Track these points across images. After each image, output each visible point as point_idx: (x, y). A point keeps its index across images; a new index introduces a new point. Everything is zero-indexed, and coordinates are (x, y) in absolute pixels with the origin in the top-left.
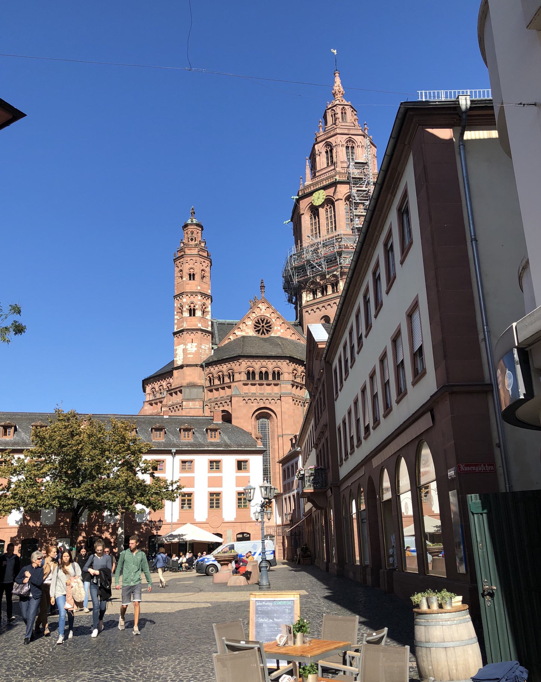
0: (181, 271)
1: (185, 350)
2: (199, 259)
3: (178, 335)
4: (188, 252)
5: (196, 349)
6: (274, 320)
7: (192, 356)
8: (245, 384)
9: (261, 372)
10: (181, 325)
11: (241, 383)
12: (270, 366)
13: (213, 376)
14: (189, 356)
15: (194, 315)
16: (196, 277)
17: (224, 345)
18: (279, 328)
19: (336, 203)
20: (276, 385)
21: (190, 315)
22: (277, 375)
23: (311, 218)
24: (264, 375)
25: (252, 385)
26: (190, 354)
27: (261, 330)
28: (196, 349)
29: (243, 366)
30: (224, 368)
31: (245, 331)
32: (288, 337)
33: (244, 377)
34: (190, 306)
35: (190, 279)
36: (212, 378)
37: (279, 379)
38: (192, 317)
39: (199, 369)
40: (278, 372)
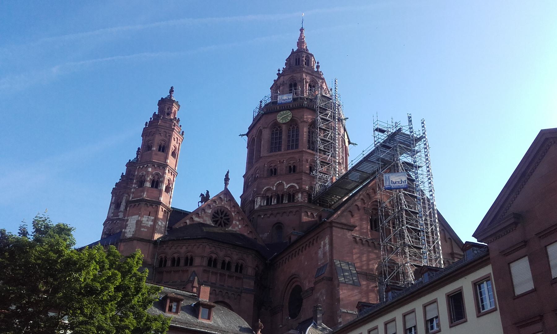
1: (139, 223)
5: (151, 223)
6: (233, 214)
7: (146, 230)
8: (205, 271)
9: (224, 262)
12: (235, 256)
14: (142, 229)
17: (180, 228)
18: (238, 223)
20: (238, 278)
21: (152, 186)
22: (240, 268)
24: (226, 266)
25: (213, 273)
26: (144, 227)
28: (152, 223)
31: (202, 218)
32: (245, 234)
34: (154, 177)
35: (159, 150)
37: (241, 272)
38: (154, 189)
39: (152, 245)
40: (242, 265)
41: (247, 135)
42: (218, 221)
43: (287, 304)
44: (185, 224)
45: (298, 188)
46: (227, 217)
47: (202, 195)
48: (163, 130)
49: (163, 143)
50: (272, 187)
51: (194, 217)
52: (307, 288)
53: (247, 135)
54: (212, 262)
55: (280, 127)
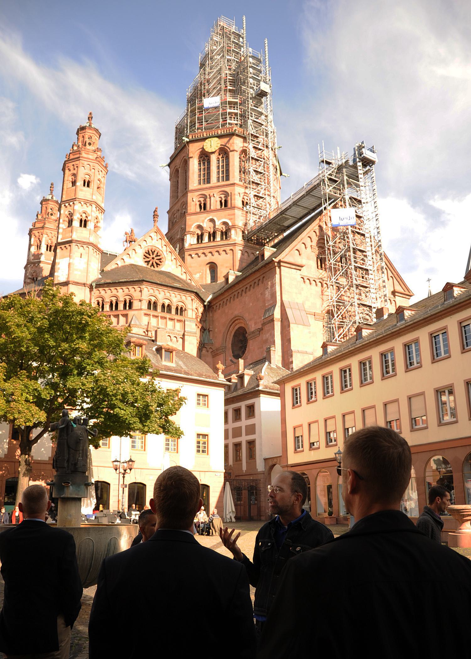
0: (74, 175)
2: (98, 167)
3: (63, 246)
4: (84, 155)
8: (146, 314)
10: (67, 235)
11: (142, 312)
12: (176, 298)
13: (103, 301)
15: (85, 226)
16: (91, 185)
17: (112, 270)
19: (231, 154)
22: (180, 311)
23: (200, 164)
24: (167, 308)
25: (153, 316)
27: (151, 263)
29: (147, 292)
30: (121, 293)
33: (145, 306)
35: (84, 185)
36: (101, 302)
37: (181, 314)
38: (83, 228)
41: (169, 165)
42: (149, 261)
43: (230, 345)
44: (117, 266)
45: (230, 224)
46: (159, 258)
47: (126, 234)
48: (86, 163)
49: (87, 176)
50: (201, 224)
51: (124, 257)
52: (253, 330)
53: (169, 165)
54: (152, 305)
55: (207, 156)
